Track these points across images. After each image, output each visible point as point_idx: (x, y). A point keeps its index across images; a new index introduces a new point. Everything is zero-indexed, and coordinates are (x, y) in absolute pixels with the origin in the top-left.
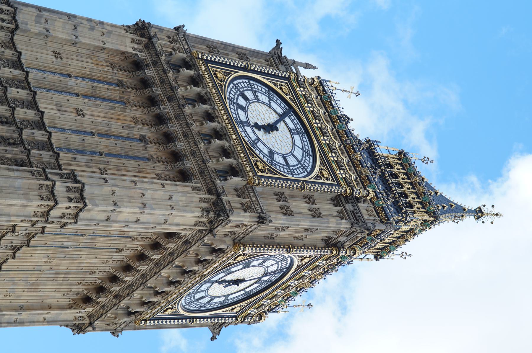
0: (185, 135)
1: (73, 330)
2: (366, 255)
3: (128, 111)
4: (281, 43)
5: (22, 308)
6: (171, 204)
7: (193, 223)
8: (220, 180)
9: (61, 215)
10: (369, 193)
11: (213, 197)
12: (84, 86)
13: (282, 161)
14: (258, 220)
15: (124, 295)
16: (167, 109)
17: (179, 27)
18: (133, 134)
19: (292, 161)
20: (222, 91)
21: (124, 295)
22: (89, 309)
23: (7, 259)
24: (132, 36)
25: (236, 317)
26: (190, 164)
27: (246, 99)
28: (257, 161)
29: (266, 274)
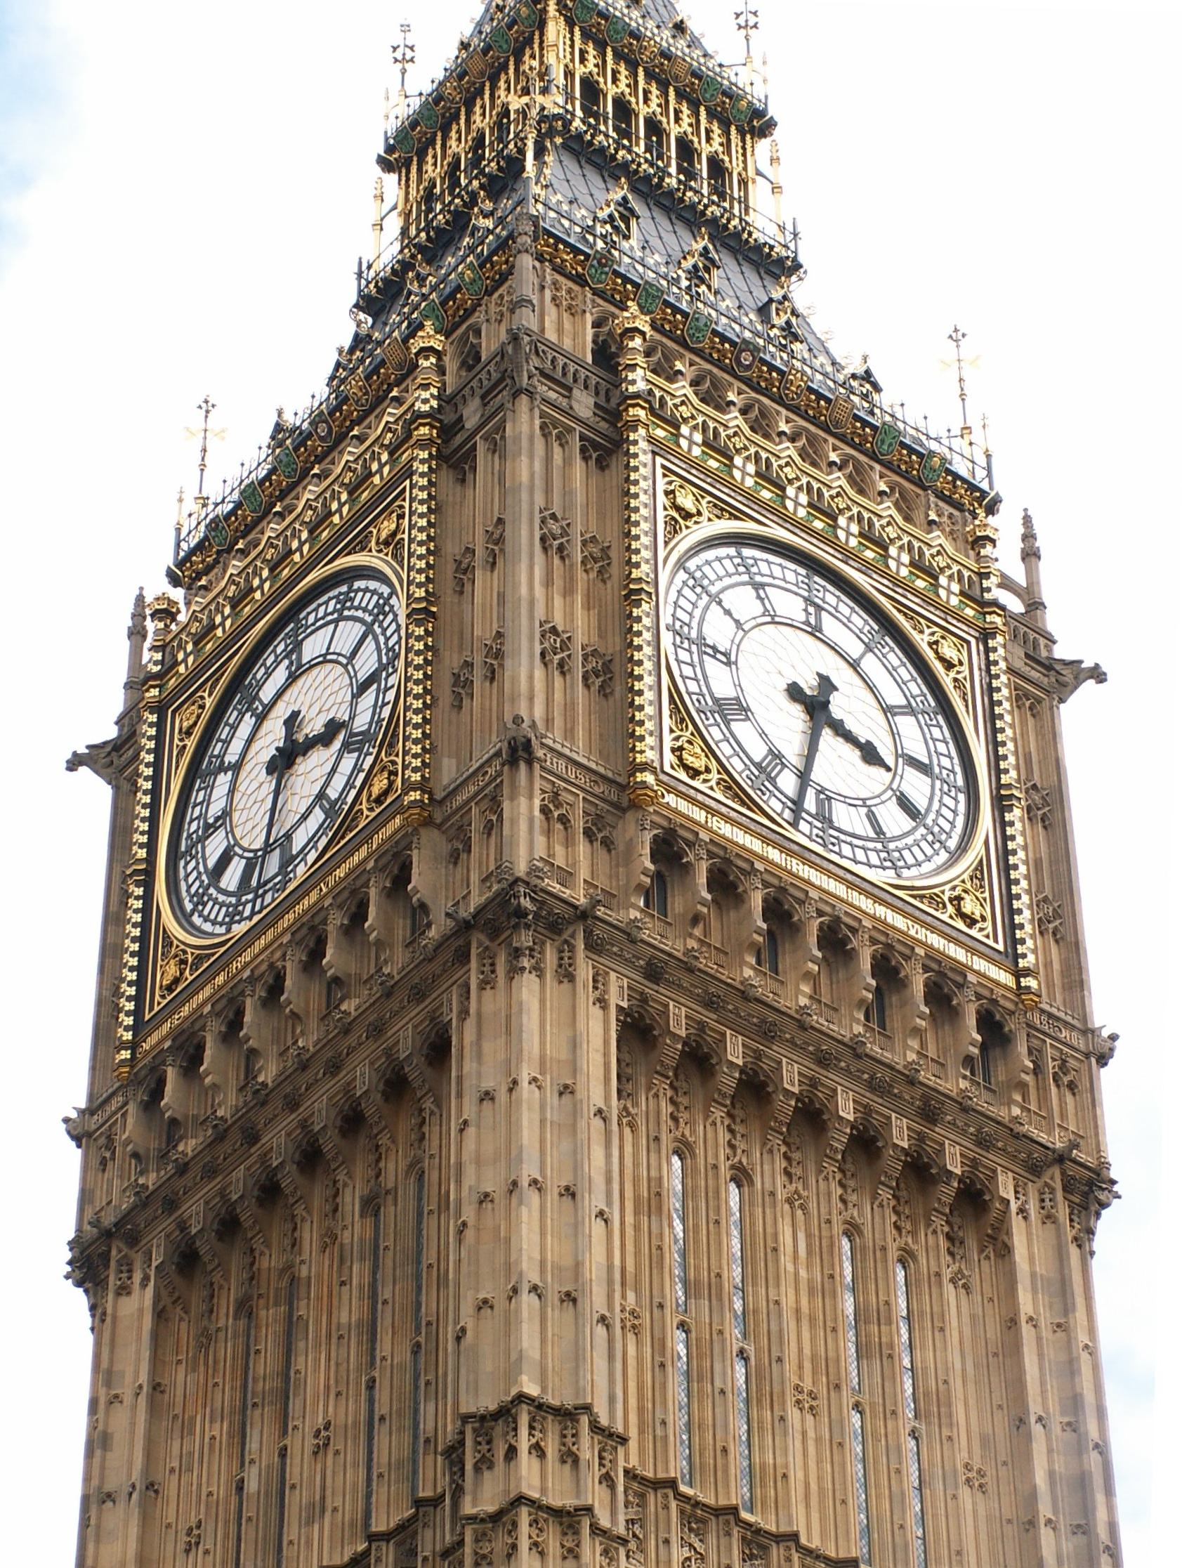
0: (334, 1067)
1: (1104, 1205)
2: (759, 173)
3: (304, 1272)
4: (75, 754)
5: (1021, 1422)
6: (503, 1089)
7: (566, 986)
8: (429, 925)
9: (567, 1467)
10: (422, 350)
11: (477, 940)
12: (260, 1440)
13: (369, 698)
14: (523, 766)
15: (919, 1092)
16: (278, 1140)
17: (69, 1133)
18: (361, 1239)
19: (367, 662)
20: (209, 956)
21: (919, 1092)
22: (1005, 1186)
23: (808, 1552)
24: (111, 1296)
25: (986, 635)
26: (406, 1036)
27: (225, 860)
28: (368, 800)
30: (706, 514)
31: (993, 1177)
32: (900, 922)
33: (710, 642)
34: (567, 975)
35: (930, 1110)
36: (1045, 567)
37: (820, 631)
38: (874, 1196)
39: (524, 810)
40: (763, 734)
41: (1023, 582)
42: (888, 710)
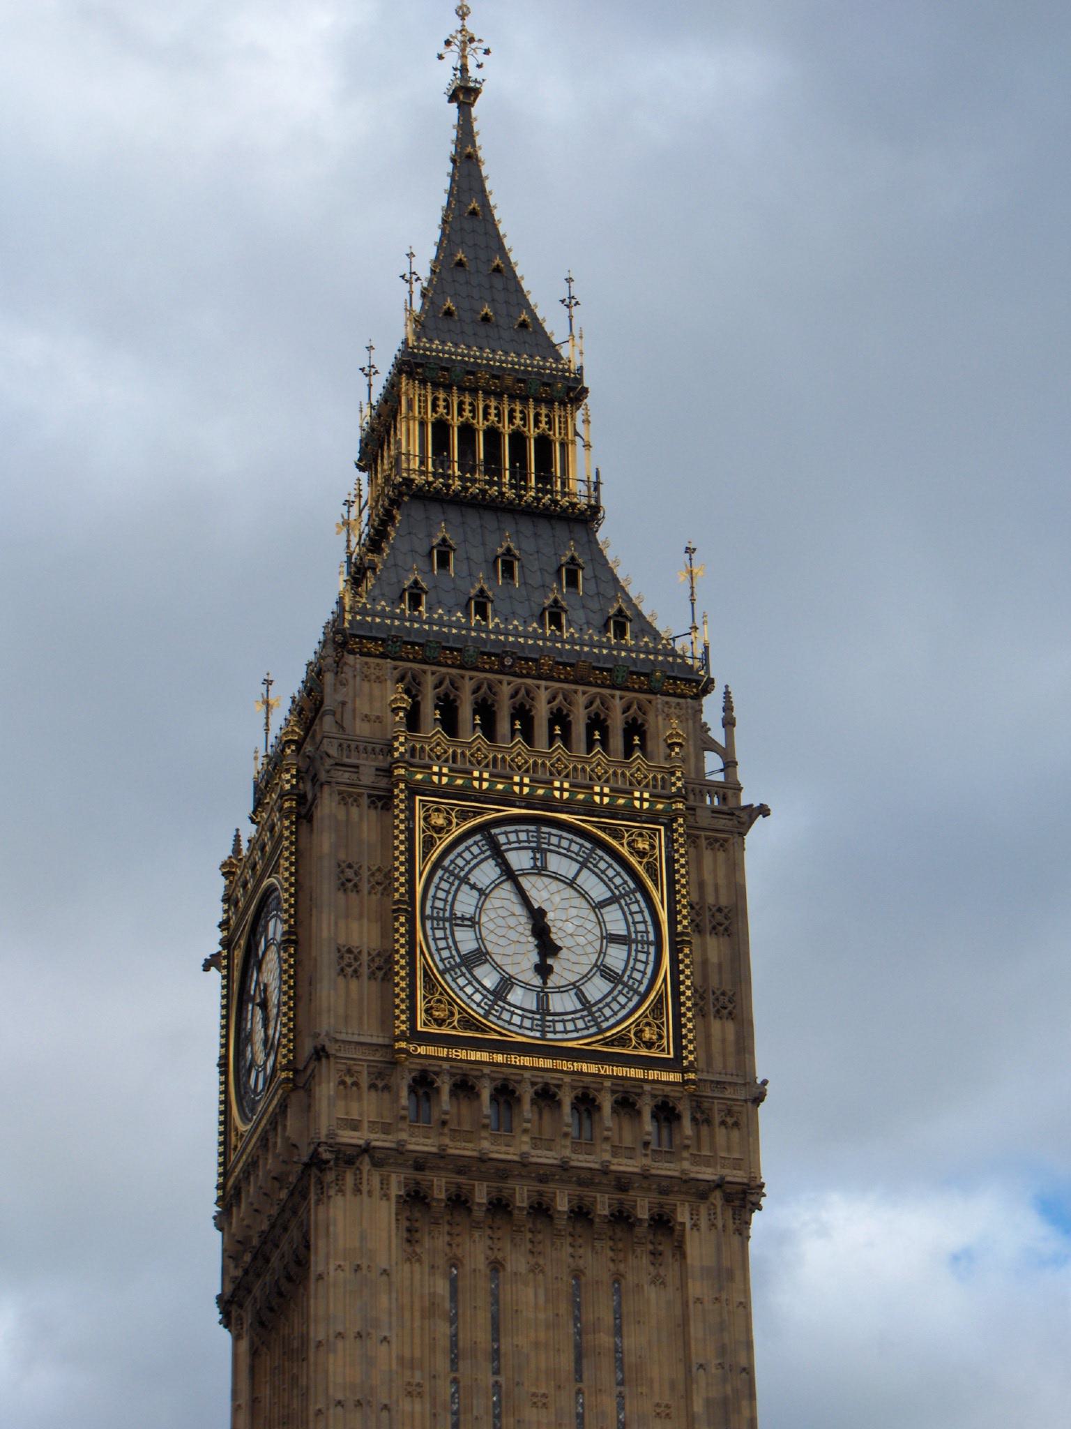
0: (285, 1229)
2: (576, 434)
11: (314, 1171)
14: (324, 1060)
30: (455, 820)
31: (674, 1211)
32: (593, 1069)
33: (459, 915)
34: (358, 1190)
35: (622, 1183)
37: (545, 868)
38: (593, 1247)
39: (326, 1089)
40: (497, 967)
41: (722, 742)
42: (598, 906)
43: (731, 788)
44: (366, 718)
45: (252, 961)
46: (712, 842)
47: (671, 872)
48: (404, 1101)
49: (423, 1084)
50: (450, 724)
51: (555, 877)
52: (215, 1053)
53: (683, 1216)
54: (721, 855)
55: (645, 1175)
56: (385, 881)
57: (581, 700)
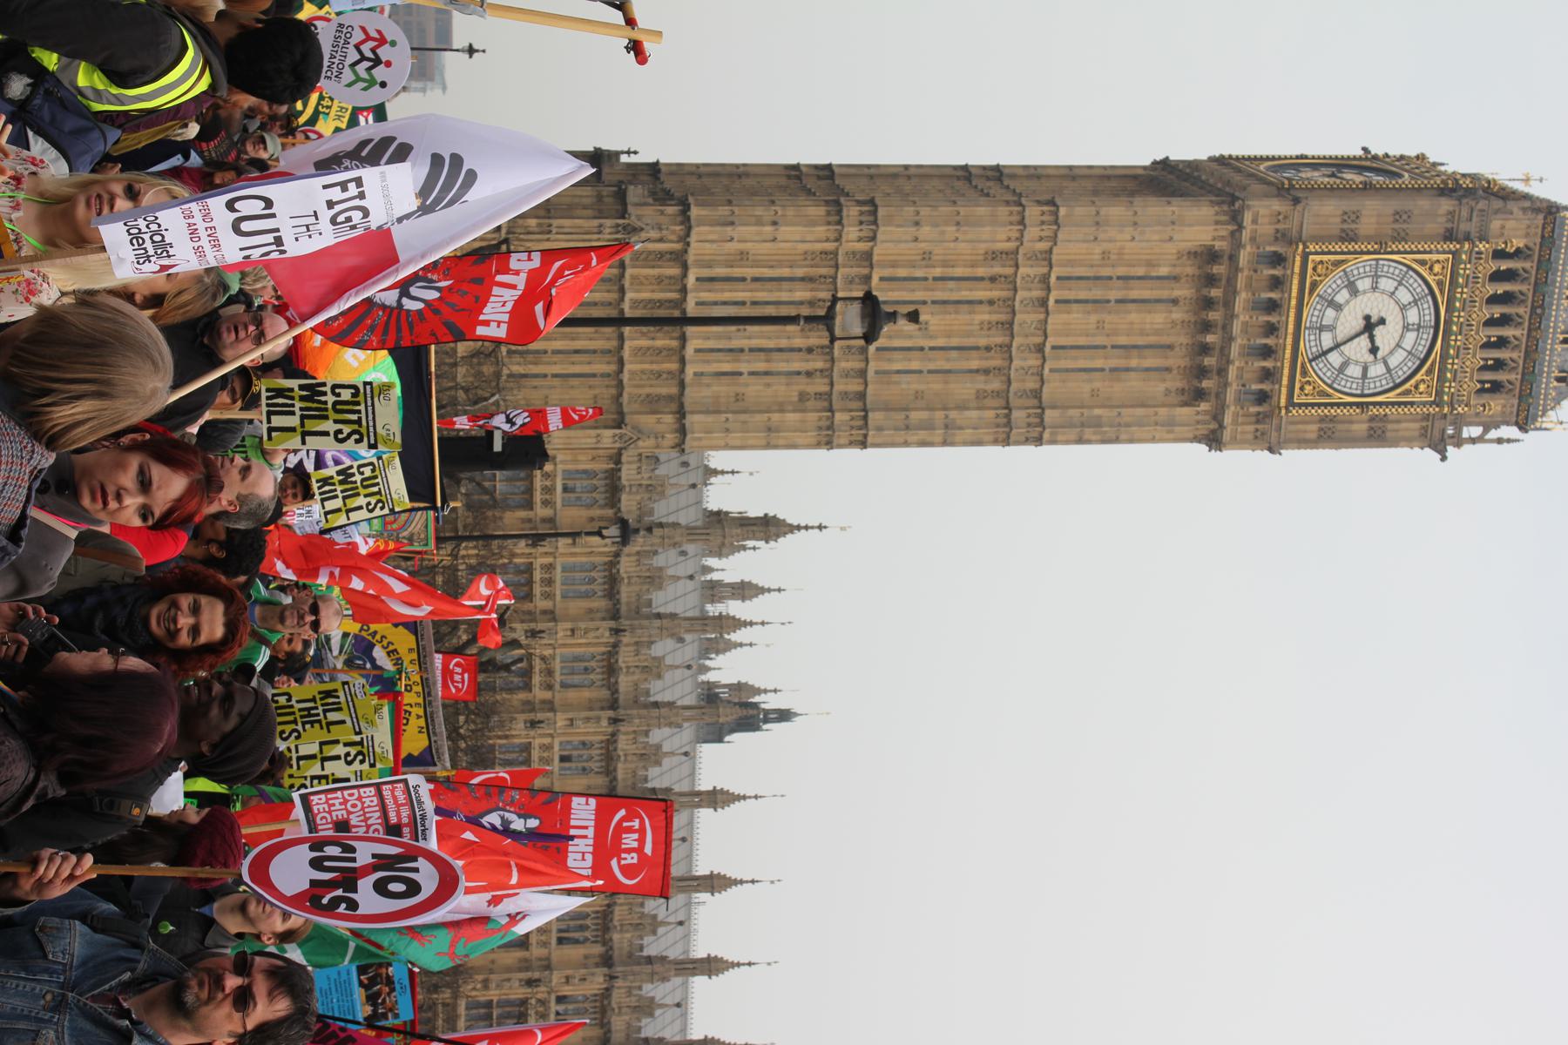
29: (1403, 308)
34: (1217, 223)
35: (1222, 372)
36: (1495, 445)
39: (1277, 205)
40: (1348, 302)
43: (1459, 442)
44: (1503, 227)
45: (1361, 169)
46: (1425, 429)
47: (1405, 404)
48: (1268, 249)
49: (1278, 260)
50: (1497, 277)
51: (1402, 336)
52: (1309, 153)
53: (1204, 406)
54: (1417, 433)
55: (1226, 385)
56: (1400, 237)
57: (1515, 355)
